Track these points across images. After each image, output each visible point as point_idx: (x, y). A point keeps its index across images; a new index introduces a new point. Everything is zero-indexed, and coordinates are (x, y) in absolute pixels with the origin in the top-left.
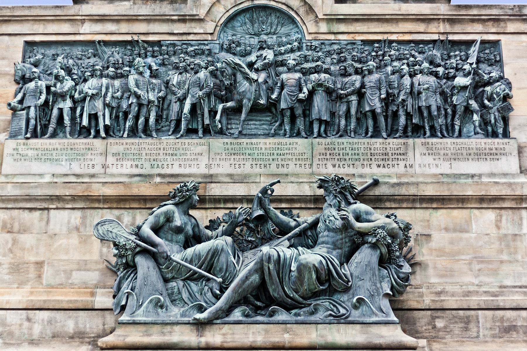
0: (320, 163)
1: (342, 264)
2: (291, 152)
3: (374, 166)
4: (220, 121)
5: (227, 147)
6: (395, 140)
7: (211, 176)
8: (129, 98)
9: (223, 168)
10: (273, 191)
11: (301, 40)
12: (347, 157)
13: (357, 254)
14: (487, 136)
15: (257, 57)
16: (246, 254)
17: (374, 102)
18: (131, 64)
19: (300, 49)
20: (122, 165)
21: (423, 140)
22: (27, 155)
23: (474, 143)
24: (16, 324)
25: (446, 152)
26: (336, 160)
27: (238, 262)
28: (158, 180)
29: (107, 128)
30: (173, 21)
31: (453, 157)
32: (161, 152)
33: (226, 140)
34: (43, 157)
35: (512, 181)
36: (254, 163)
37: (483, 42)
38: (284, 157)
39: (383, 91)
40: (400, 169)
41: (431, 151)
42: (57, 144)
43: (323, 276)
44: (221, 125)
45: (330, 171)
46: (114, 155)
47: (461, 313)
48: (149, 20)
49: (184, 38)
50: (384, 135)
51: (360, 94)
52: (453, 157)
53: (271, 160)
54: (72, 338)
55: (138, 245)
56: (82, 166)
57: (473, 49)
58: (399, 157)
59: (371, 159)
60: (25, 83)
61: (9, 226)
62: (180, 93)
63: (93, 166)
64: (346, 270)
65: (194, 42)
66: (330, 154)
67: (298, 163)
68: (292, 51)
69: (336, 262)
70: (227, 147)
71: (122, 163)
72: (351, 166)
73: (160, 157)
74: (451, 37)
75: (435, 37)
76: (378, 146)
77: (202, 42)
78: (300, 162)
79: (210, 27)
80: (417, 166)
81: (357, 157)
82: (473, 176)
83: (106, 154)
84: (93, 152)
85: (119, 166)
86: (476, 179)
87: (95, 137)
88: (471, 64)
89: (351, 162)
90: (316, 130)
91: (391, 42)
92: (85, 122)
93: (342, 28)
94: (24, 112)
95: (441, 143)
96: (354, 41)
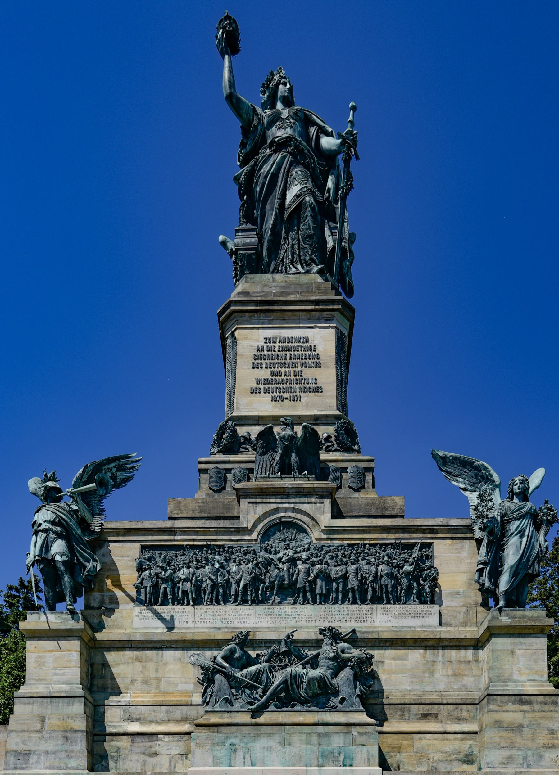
0: (321, 620)
1: (332, 678)
7: (257, 628)
8: (206, 581)
9: (263, 623)
10: (293, 636)
12: (337, 616)
13: (341, 672)
14: (421, 603)
16: (277, 673)
17: (353, 583)
18: (207, 559)
19: (308, 549)
21: (382, 606)
22: (147, 616)
24: (147, 713)
25: (396, 613)
27: (273, 678)
28: (226, 630)
31: (400, 616)
32: (227, 614)
33: (265, 606)
35: (434, 630)
39: (359, 576)
40: (368, 624)
43: (322, 684)
45: (327, 625)
47: (400, 706)
48: (218, 531)
49: (239, 543)
50: (359, 602)
51: (345, 577)
52: (400, 616)
54: (180, 721)
55: (215, 667)
56: (181, 622)
57: (415, 548)
58: (368, 616)
60: (142, 572)
61: (140, 658)
62: (237, 577)
63: (187, 622)
64: (334, 682)
67: (308, 620)
68: (304, 551)
69: (329, 677)
74: (402, 541)
76: (355, 609)
79: (255, 535)
81: (342, 616)
86: (413, 629)
87: (187, 605)
88: (414, 558)
90: (318, 601)
91: (365, 544)
92: (180, 596)
94: (144, 589)
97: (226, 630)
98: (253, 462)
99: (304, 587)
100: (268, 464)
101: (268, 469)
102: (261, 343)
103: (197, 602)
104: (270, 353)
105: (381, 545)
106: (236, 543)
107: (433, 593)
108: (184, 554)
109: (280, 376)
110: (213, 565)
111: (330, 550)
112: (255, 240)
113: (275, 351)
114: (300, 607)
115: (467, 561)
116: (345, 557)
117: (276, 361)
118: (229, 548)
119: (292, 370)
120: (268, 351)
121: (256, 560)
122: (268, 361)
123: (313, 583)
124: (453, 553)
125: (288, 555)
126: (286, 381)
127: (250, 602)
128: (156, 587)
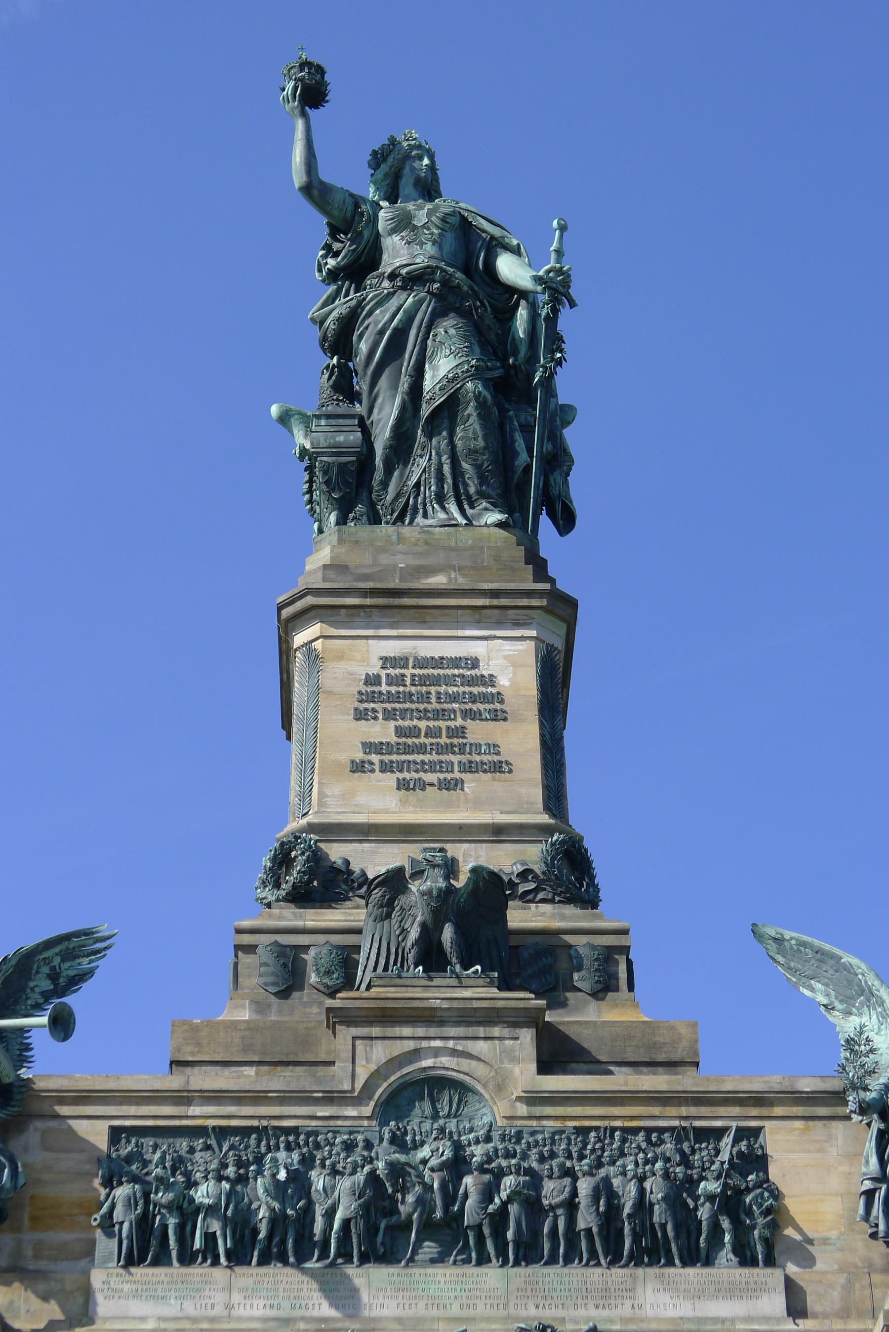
0: (519, 1302)
2: (479, 1286)
3: (591, 1307)
4: (382, 1243)
5: (393, 1279)
6: (619, 1271)
11: (491, 1126)
15: (432, 1152)
19: (488, 1139)
20: (252, 1306)
23: (725, 1274)
26: (540, 1298)
28: (302, 1326)
29: (229, 1254)
30: (316, 1102)
34: (145, 1294)
36: (430, 1302)
37: (739, 1130)
38: (470, 1294)
40: (626, 1310)
41: (668, 1286)
42: (163, 1275)
44: (385, 1248)
46: (241, 1290)
48: (284, 1098)
51: (571, 1205)
53: (452, 1298)
56: (198, 1306)
58: (625, 1294)
59: (587, 1297)
60: (112, 1188)
63: (213, 1306)
65: (344, 1129)
66: (532, 1290)
67: (489, 1302)
68: (477, 1142)
70: (393, 1279)
71: (251, 1301)
72: (560, 1307)
73: (303, 1294)
74: (697, 1124)
75: (676, 1123)
77: (356, 1129)
78: (492, 1301)
80: (648, 1306)
82: (723, 1321)
83: (229, 1289)
84: (212, 1287)
85: (248, 1306)
88: (723, 1163)
89: (560, 1302)
91: (614, 1130)
92: (198, 1244)
93: (549, 1110)
95: (681, 1275)
96: (564, 1129)
97: (302, 1326)
98: (359, 931)
99: (479, 1226)
100: (393, 939)
101: (393, 950)
102: (375, 668)
103: (238, 1257)
104: (393, 689)
105: (649, 1131)
106: (326, 1123)
107: (769, 1245)
108: (208, 1147)
109: (418, 736)
110: (274, 1176)
111: (537, 1142)
112: (356, 437)
113: (405, 685)
114: (471, 1270)
115: (841, 1169)
116: (570, 1157)
117: (408, 705)
118: (308, 1134)
119: (442, 724)
120: (389, 684)
121: (371, 1162)
122: (388, 706)
123: (500, 1219)
124: (809, 1151)
125: (442, 1154)
126: (428, 748)
127: (355, 1259)
128: (144, 1223)
